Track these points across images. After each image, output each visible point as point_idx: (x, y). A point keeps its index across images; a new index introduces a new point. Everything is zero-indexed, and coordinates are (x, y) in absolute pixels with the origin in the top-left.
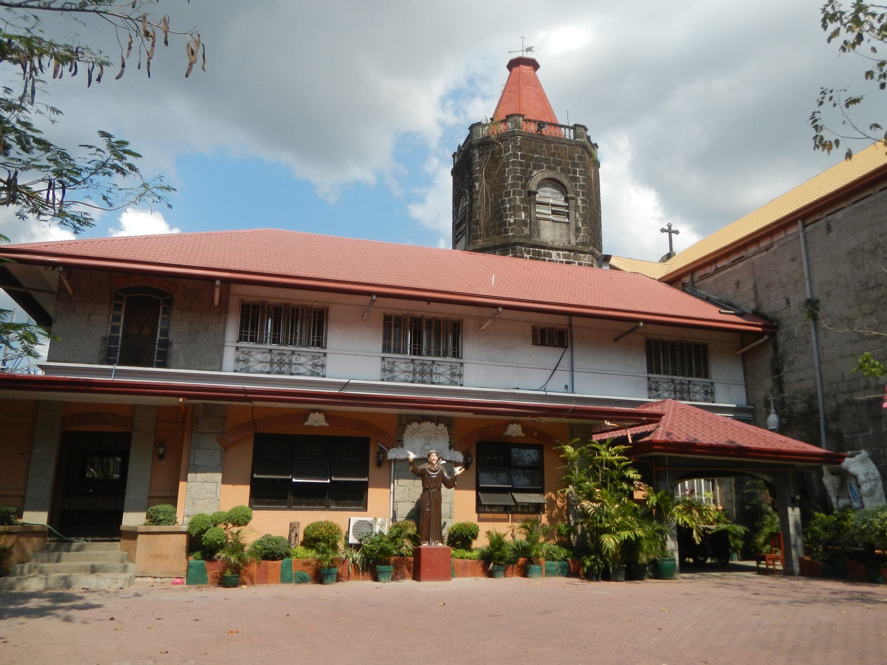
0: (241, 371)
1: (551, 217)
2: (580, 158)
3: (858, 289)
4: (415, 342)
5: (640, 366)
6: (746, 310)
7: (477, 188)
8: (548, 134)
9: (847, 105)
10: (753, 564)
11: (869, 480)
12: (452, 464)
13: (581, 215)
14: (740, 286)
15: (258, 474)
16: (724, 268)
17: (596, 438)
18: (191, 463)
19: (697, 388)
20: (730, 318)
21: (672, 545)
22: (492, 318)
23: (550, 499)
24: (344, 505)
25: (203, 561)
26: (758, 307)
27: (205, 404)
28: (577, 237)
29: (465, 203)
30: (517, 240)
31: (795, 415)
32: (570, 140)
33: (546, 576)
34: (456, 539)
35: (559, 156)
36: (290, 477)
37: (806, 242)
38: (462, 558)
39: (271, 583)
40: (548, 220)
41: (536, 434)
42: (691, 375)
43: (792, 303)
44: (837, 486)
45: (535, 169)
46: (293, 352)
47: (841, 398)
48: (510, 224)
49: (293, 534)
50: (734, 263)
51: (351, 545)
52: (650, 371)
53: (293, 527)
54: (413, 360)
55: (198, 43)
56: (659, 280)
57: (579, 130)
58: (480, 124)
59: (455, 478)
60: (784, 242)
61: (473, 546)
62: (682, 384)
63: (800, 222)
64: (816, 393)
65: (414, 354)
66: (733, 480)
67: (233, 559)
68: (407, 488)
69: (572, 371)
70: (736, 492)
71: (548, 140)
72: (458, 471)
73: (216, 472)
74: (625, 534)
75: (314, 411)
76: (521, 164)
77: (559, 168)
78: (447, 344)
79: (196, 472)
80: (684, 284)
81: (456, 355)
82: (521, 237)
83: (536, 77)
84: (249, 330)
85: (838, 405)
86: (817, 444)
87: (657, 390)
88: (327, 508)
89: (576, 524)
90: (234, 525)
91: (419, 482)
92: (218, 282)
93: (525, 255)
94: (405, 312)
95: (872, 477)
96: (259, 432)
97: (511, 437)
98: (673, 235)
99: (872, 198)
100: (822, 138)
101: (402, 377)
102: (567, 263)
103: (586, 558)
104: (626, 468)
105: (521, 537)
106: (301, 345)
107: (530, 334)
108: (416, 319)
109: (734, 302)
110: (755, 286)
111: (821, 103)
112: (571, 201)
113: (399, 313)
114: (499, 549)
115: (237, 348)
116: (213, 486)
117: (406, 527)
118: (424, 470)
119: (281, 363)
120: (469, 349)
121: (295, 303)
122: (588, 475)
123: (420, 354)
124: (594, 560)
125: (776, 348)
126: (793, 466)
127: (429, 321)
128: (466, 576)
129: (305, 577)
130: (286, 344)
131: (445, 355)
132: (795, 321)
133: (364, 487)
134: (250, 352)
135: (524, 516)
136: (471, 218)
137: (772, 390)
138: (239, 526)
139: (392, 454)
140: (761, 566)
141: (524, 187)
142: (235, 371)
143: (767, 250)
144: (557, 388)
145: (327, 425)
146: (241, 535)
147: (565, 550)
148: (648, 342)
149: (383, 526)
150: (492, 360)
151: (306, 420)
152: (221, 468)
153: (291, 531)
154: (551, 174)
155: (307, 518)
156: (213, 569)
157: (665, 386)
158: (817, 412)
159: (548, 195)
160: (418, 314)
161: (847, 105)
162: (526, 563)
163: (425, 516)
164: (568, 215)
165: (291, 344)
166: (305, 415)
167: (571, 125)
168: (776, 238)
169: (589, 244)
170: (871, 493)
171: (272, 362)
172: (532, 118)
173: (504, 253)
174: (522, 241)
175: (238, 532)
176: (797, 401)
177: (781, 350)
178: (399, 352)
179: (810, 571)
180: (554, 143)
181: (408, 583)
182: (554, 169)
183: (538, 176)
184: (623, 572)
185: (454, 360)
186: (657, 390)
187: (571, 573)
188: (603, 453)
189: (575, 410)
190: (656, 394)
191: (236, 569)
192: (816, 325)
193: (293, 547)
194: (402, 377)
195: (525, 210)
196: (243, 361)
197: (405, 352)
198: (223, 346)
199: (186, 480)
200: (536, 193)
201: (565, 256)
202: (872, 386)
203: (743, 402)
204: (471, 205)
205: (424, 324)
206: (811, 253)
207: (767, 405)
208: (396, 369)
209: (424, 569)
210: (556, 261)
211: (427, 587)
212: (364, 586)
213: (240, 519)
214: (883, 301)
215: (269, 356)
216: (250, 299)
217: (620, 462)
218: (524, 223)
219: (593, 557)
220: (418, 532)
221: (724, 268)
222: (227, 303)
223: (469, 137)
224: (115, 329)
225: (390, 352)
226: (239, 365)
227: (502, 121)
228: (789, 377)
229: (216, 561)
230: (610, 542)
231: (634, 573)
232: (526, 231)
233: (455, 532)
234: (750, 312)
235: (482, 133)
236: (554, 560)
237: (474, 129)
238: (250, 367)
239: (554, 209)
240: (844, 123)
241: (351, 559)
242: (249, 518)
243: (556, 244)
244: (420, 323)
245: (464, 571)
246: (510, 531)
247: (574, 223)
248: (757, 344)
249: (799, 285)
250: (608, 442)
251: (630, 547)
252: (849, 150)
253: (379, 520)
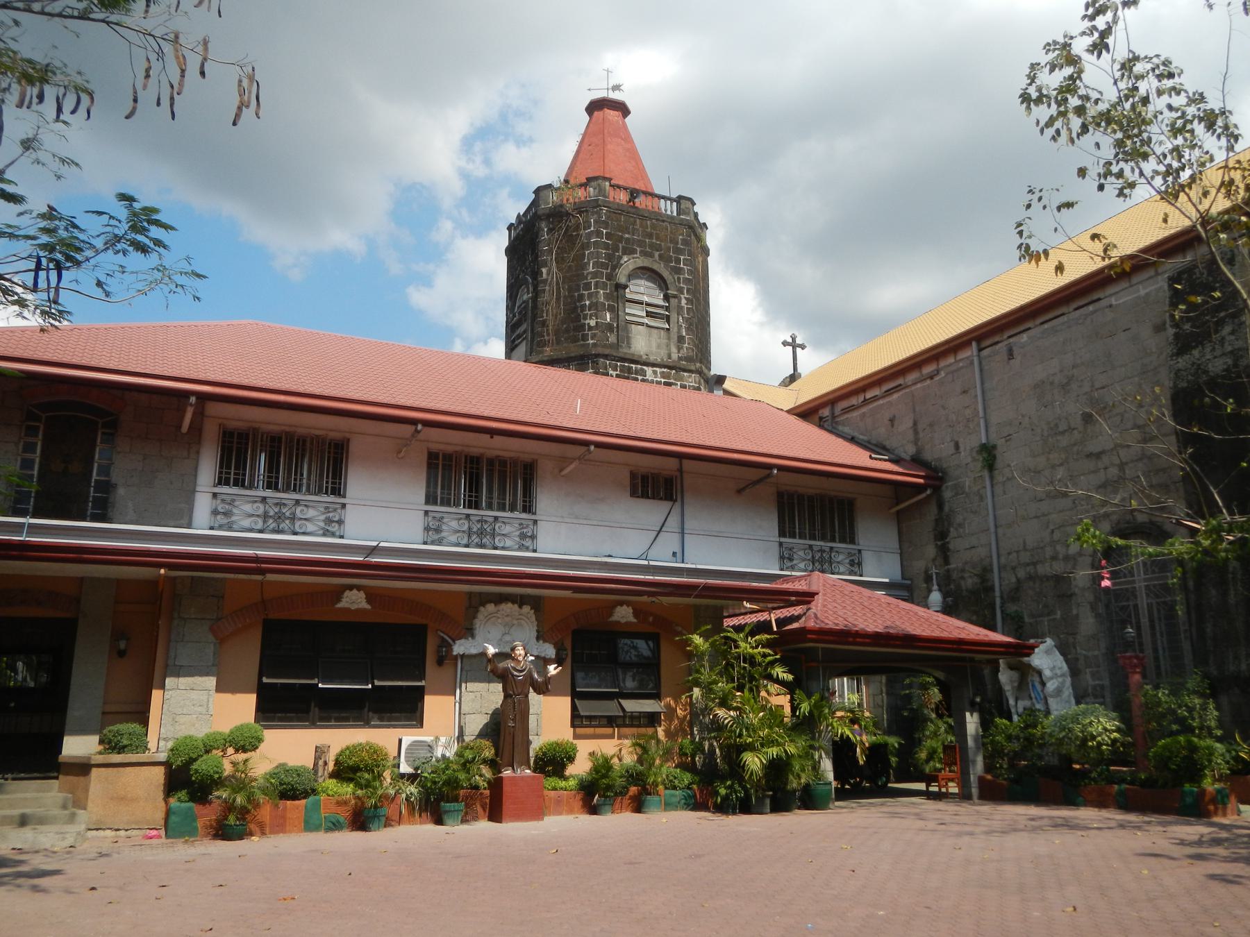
0: (221, 527)
1: (646, 321)
2: (685, 242)
3: (1046, 434)
4: (471, 491)
5: (769, 526)
6: (903, 455)
7: (545, 276)
8: (643, 206)
9: (1059, 209)
10: (921, 786)
11: (1055, 676)
12: (543, 662)
13: (686, 320)
14: (896, 423)
15: (268, 677)
16: (875, 398)
17: (729, 622)
18: (170, 662)
19: (841, 557)
20: (882, 466)
21: (827, 766)
22: (579, 458)
23: (668, 706)
25: (191, 804)
26: (919, 452)
27: (193, 578)
28: (679, 349)
29: (526, 296)
30: (600, 350)
31: (964, 593)
32: (672, 217)
33: (665, 810)
34: (546, 764)
35: (657, 239)
36: (316, 681)
37: (981, 370)
38: (555, 789)
39: (290, 832)
40: (642, 324)
41: (651, 619)
42: (833, 540)
43: (962, 449)
44: (1016, 684)
45: (624, 253)
46: (297, 502)
47: (1021, 573)
48: (590, 328)
49: (321, 763)
50: (889, 392)
51: (402, 776)
52: (782, 533)
53: (320, 752)
54: (468, 516)
55: (251, 78)
56: (788, 412)
57: (684, 204)
58: (549, 186)
59: (548, 680)
60: (953, 368)
61: (567, 773)
62: (822, 551)
63: (974, 344)
64: (991, 565)
65: (470, 507)
66: (884, 679)
67: (240, 800)
69: (683, 533)
70: (887, 694)
71: (644, 216)
72: (552, 670)
73: (207, 674)
74: (774, 751)
75: (351, 587)
76: (606, 246)
77: (657, 254)
78: (515, 495)
79: (178, 676)
80: (821, 419)
81: (528, 508)
82: (605, 346)
83: (625, 125)
84: (233, 470)
85: (1018, 580)
86: (992, 628)
87: (791, 559)
88: (367, 724)
89: (702, 739)
90: (237, 751)
92: (193, 399)
93: (611, 372)
94: (458, 448)
95: (1059, 672)
96: (271, 616)
97: (618, 622)
98: (798, 350)
99: (1065, 318)
100: (1028, 247)
101: (453, 538)
102: (665, 384)
103: (722, 784)
104: (772, 663)
105: (629, 759)
106: (309, 491)
107: (627, 482)
108: (472, 458)
109: (887, 443)
110: (915, 424)
111: (1029, 206)
112: (672, 300)
113: (450, 449)
114: (605, 776)
115: (215, 495)
116: (203, 696)
117: (481, 749)
118: (506, 670)
119: (279, 517)
120: (545, 501)
121: (301, 431)
122: (721, 674)
123: (477, 508)
124: (730, 787)
125: (940, 506)
126: (972, 660)
127: (491, 462)
128: (560, 814)
130: (287, 489)
131: (513, 509)
132: (965, 470)
133: (419, 694)
134: (234, 501)
135: (634, 730)
136: (534, 317)
137: (934, 560)
138: (245, 751)
139: (459, 648)
140: (931, 789)
141: (610, 277)
142: (212, 528)
143: (932, 378)
144: (662, 556)
145: (369, 607)
146: (250, 764)
147: (689, 775)
148: (780, 495)
149: (446, 749)
150: (577, 518)
151: (339, 600)
152: (214, 669)
153: (317, 759)
154: (645, 262)
155: (340, 739)
156: (207, 815)
157: (801, 553)
158: (992, 589)
159: (642, 290)
160: (475, 451)
161: (1059, 209)
162: (640, 794)
163: (505, 731)
164: (668, 319)
165: (294, 490)
166: (338, 592)
167: (674, 196)
168: (943, 363)
169: (693, 360)
170: (1058, 692)
171: (265, 516)
172: (621, 183)
173: (582, 368)
174: (607, 352)
175: (246, 760)
176: (966, 575)
177: (946, 509)
178: (449, 505)
179: (993, 793)
180: (651, 219)
181: (483, 827)
182: (651, 256)
183: (629, 263)
184: (768, 801)
185: (524, 516)
186: (791, 559)
187: (697, 805)
188: (742, 644)
189: (707, 588)
190: (789, 564)
191: (243, 813)
192: (992, 478)
193: (320, 780)
194: (453, 538)
195: (611, 309)
196: (222, 514)
197: (457, 505)
198: (194, 491)
199: (162, 687)
200: (626, 287)
201: (663, 375)
202: (1061, 556)
203: (897, 576)
204: (535, 299)
205: (481, 466)
206: (987, 385)
207: (928, 579)
208: (444, 527)
209: (507, 805)
210: (652, 382)
211: (512, 830)
212: (419, 834)
213: (245, 743)
214: (1075, 449)
215: (261, 506)
216: (232, 425)
217: (765, 656)
218: (610, 327)
219: (729, 783)
220: (497, 754)
221: (875, 398)
222: (200, 431)
223: (534, 204)
224: (27, 464)
225: (435, 503)
226: (216, 519)
227: (581, 185)
228: (954, 544)
229: (210, 803)
230: (754, 762)
231: (781, 804)
232: (612, 339)
233: (545, 754)
234: (908, 458)
235: (553, 199)
236: (675, 788)
237: (542, 194)
238: (233, 522)
239: (650, 309)
240: (1056, 230)
241: (404, 796)
242: (260, 740)
243: (652, 358)
244: (478, 463)
245: (559, 807)
246: (617, 749)
247: (676, 330)
248: (917, 501)
249: (971, 426)
250: (747, 629)
251: (777, 768)
252: (1060, 262)
253: (443, 739)
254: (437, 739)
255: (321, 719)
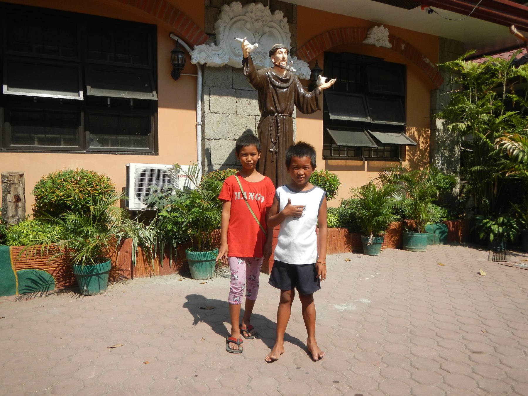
24: (115, 143)
41: (403, 47)
49: (10, 198)
51: (133, 214)
68: (224, 116)
88: (84, 148)
91: (255, 103)
97: (374, 46)
129: (42, 279)
133: (152, 108)
139: (200, 55)
149: (188, 178)
193: (12, 221)
241: (136, 241)
253: (185, 168)
254: (177, 167)
255: (17, 140)
